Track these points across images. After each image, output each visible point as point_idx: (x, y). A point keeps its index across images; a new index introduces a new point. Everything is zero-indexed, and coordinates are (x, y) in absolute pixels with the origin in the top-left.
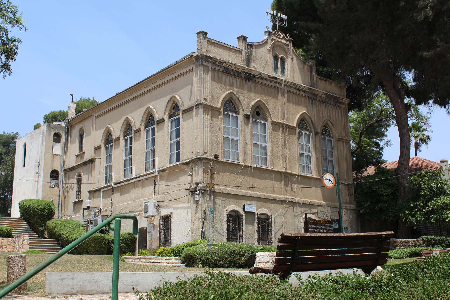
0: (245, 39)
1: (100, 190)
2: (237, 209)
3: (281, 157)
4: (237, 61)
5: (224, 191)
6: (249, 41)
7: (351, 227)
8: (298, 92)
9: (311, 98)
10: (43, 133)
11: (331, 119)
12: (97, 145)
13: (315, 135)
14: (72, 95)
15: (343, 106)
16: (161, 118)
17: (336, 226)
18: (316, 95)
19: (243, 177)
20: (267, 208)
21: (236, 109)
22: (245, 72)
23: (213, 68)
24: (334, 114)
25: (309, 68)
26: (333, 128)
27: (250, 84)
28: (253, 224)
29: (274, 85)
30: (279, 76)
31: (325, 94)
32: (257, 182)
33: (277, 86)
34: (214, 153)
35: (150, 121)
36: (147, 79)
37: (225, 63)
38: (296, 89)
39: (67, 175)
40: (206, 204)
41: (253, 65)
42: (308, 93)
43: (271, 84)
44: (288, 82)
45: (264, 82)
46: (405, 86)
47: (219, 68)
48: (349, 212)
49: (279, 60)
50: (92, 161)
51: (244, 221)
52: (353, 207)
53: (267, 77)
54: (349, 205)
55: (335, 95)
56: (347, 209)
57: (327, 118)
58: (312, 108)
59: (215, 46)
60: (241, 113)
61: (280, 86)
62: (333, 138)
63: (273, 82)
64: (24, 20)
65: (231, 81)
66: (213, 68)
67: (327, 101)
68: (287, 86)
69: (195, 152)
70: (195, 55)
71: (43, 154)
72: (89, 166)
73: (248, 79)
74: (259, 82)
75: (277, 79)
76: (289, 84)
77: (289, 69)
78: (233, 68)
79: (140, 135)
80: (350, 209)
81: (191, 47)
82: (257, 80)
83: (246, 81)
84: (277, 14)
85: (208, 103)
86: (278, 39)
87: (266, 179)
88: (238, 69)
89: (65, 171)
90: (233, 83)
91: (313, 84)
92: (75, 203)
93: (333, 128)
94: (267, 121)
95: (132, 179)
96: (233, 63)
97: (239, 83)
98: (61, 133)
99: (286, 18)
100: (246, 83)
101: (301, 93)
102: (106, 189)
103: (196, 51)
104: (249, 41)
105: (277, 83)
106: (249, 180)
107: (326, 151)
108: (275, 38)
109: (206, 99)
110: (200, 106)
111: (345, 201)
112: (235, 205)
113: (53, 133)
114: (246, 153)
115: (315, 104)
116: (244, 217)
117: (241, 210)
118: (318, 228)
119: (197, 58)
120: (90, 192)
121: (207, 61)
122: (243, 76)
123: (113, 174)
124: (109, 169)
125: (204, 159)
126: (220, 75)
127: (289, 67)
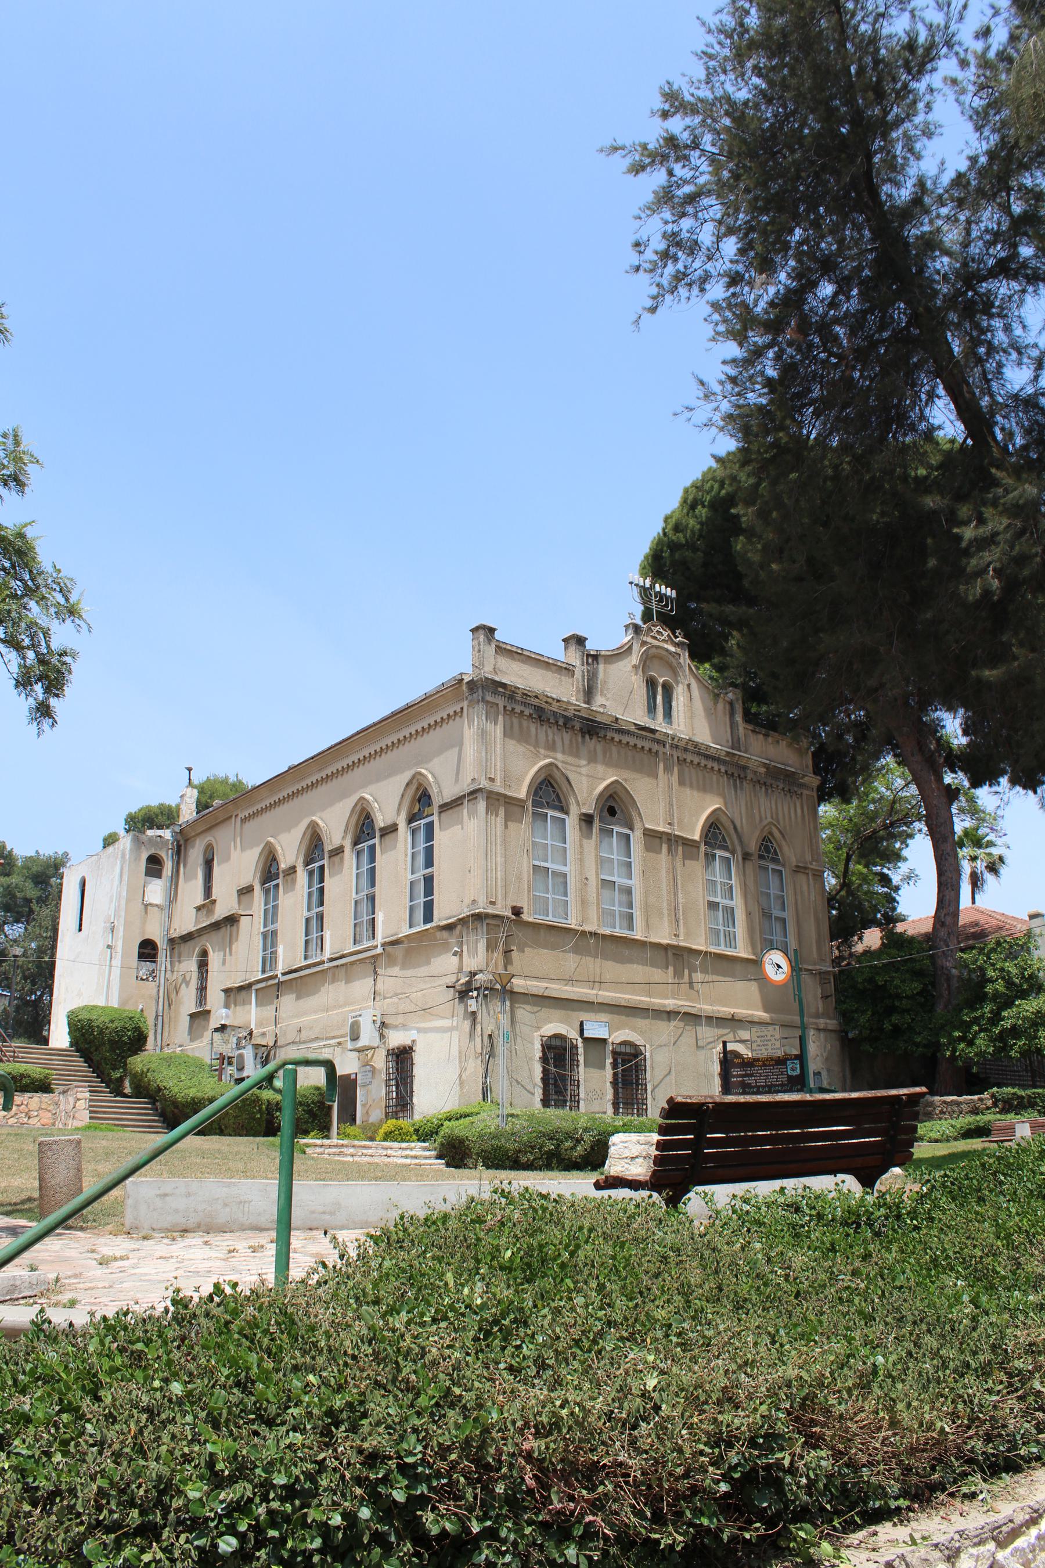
0: (580, 641)
1: (250, 986)
2: (564, 1033)
3: (666, 912)
4: (565, 692)
6: (591, 646)
7: (828, 1070)
8: (703, 762)
10: (123, 855)
12: (244, 884)
13: (744, 859)
14: (190, 770)
15: (805, 792)
16: (389, 822)
17: (793, 1069)
18: (745, 768)
21: (560, 801)
22: (582, 718)
23: (509, 708)
25: (728, 706)
26: (783, 843)
27: (592, 743)
28: (602, 1067)
29: (647, 745)
30: (658, 724)
31: (765, 765)
32: (611, 969)
33: (655, 747)
35: (364, 828)
36: (358, 733)
38: (699, 754)
39: (176, 951)
40: (493, 1021)
41: (599, 700)
42: (725, 762)
43: (640, 743)
44: (680, 739)
45: (625, 739)
46: (943, 744)
47: (522, 708)
48: (822, 1035)
49: (660, 689)
50: (232, 920)
52: (832, 1024)
53: (632, 728)
54: (822, 1021)
56: (819, 1030)
57: (769, 819)
59: (514, 659)
60: (574, 810)
61: (661, 749)
62: (783, 865)
63: (644, 738)
64: (86, 608)
65: (550, 738)
66: (509, 708)
67: (769, 781)
68: (677, 747)
69: (467, 901)
70: (467, 679)
71: (123, 902)
72: (225, 931)
73: (589, 732)
75: (653, 731)
76: (682, 744)
77: (681, 708)
78: (555, 707)
79: (342, 859)
80: (825, 1030)
81: (460, 660)
82: (609, 735)
83: (583, 737)
84: (652, 586)
85: (498, 787)
86: (655, 642)
87: (630, 961)
88: (566, 710)
89: (172, 941)
91: (736, 744)
92: (192, 1016)
93: (783, 843)
94: (632, 829)
95: (323, 962)
97: (567, 742)
98: (163, 855)
99: (674, 594)
100: (583, 742)
101: (710, 764)
102: (263, 985)
103: (469, 670)
104: (591, 646)
105: (654, 740)
106: (592, 965)
107: (768, 895)
108: (649, 640)
109: (492, 780)
110: (479, 795)
111: (813, 1010)
113: (145, 856)
114: (584, 903)
115: (742, 789)
116: (581, 1051)
117: (573, 1034)
118: (751, 1075)
119: (472, 684)
120: (227, 991)
121: (495, 693)
122: (578, 726)
123: (280, 950)
124: (270, 938)
125: (487, 916)
126: (525, 723)
127: (681, 704)
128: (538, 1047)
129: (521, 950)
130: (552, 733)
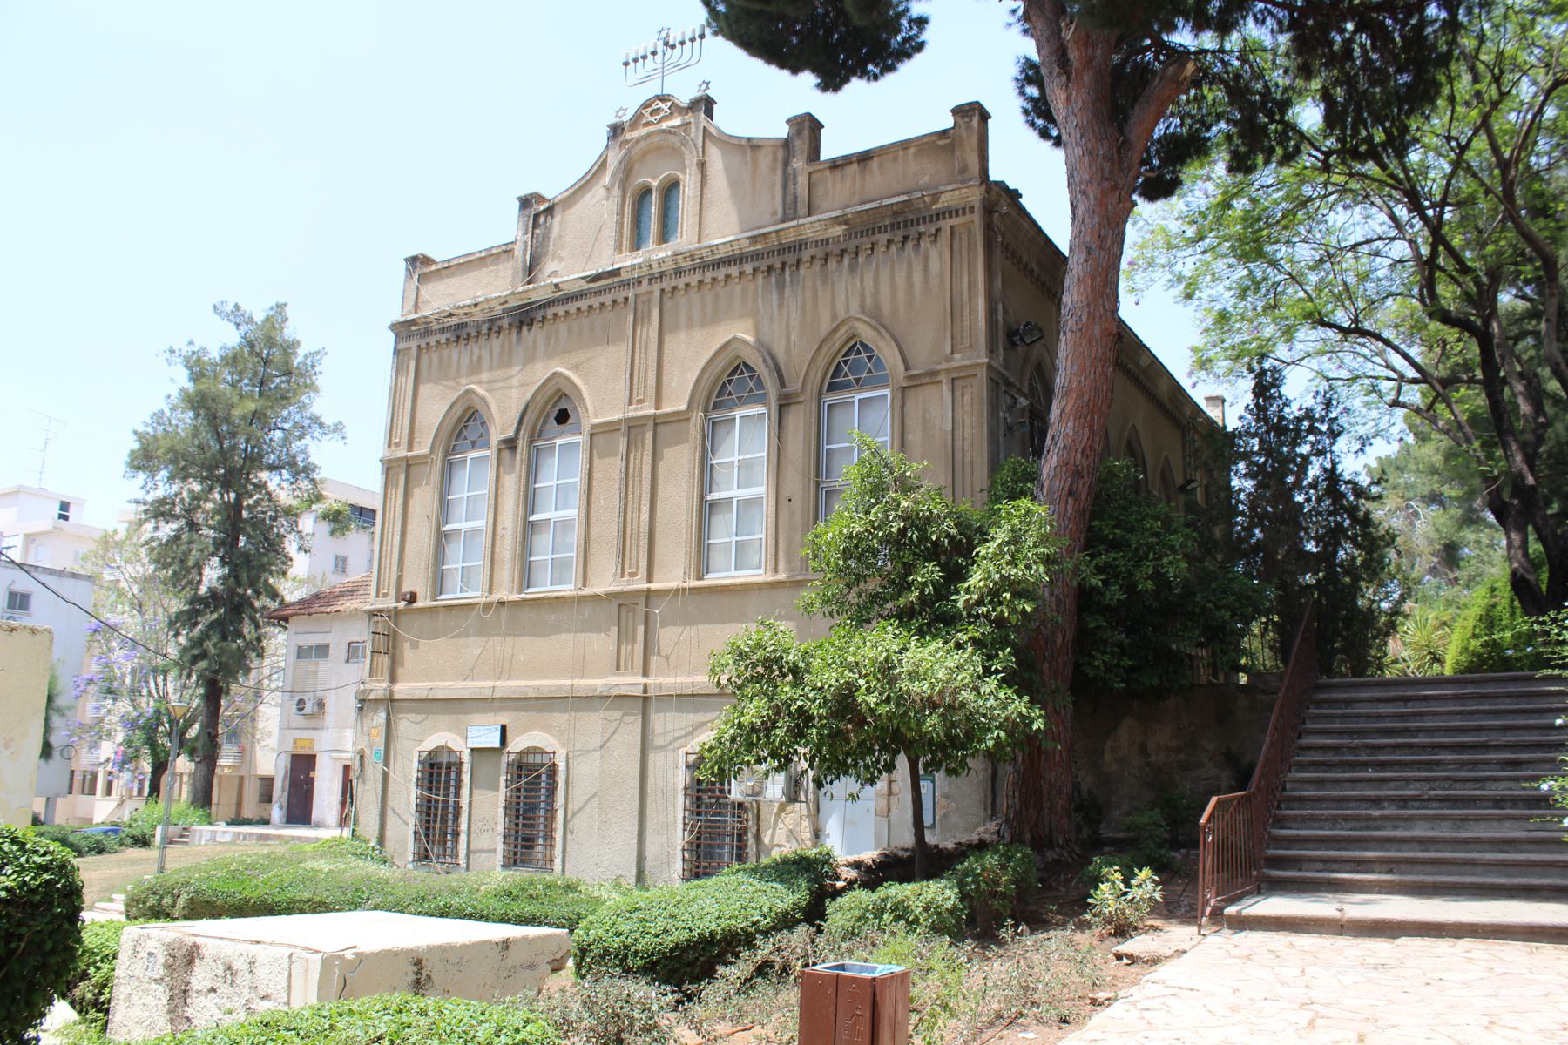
5: (418, 695)
8: (709, 275)
9: (770, 269)
11: (877, 307)
18: (799, 246)
19: (481, 641)
20: (547, 729)
24: (900, 276)
28: (497, 788)
32: (528, 647)
34: (406, 588)
37: (451, 315)
38: (703, 267)
42: (755, 256)
43: (595, 301)
45: (572, 307)
51: (466, 777)
53: (586, 286)
55: (886, 202)
58: (781, 305)
63: (606, 290)
65: (475, 358)
68: (662, 275)
74: (556, 315)
76: (668, 266)
78: (478, 315)
88: (491, 310)
90: (480, 358)
96: (468, 302)
101: (723, 271)
106: (499, 646)
112: (449, 730)
116: (466, 767)
122: (505, 323)
126: (446, 353)
128: (416, 764)
129: (415, 646)
130: (478, 349)
